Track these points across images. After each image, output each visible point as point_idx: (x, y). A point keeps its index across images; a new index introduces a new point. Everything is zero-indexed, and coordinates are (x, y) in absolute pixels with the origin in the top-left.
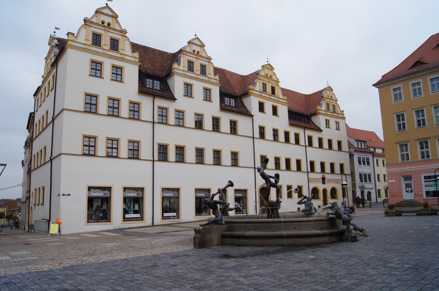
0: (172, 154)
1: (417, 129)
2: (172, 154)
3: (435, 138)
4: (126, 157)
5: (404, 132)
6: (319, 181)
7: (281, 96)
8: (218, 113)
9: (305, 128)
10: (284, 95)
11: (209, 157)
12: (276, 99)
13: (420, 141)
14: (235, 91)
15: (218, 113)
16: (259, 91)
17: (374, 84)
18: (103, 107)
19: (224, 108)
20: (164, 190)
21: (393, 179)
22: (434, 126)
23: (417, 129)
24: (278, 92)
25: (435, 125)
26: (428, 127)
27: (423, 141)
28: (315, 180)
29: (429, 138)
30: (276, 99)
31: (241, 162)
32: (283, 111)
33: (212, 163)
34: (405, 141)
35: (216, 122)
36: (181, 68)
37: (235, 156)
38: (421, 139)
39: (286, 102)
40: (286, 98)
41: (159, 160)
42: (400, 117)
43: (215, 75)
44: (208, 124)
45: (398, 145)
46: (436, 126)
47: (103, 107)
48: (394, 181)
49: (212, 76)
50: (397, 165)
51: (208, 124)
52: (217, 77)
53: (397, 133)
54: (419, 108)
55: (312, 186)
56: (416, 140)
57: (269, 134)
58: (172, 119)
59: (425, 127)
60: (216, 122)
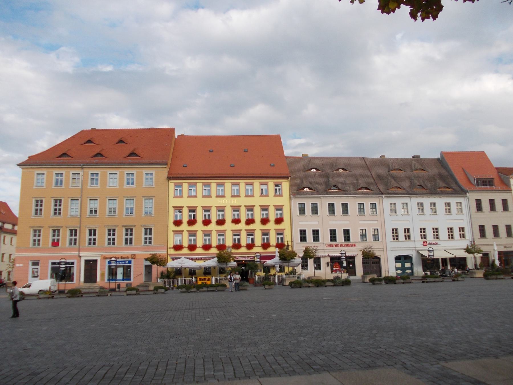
1: (52, 217)
3: (67, 227)
5: (40, 217)
13: (53, 229)
17: (18, 163)
21: (21, 264)
22: (68, 217)
23: (52, 217)
25: (69, 216)
26: (62, 217)
27: (56, 229)
29: (62, 227)
34: (39, 227)
38: (54, 227)
42: (39, 203)
45: (32, 230)
46: (69, 217)
48: (21, 265)
50: (26, 250)
53: (33, 217)
54: (57, 198)
56: (49, 227)
59: (60, 216)
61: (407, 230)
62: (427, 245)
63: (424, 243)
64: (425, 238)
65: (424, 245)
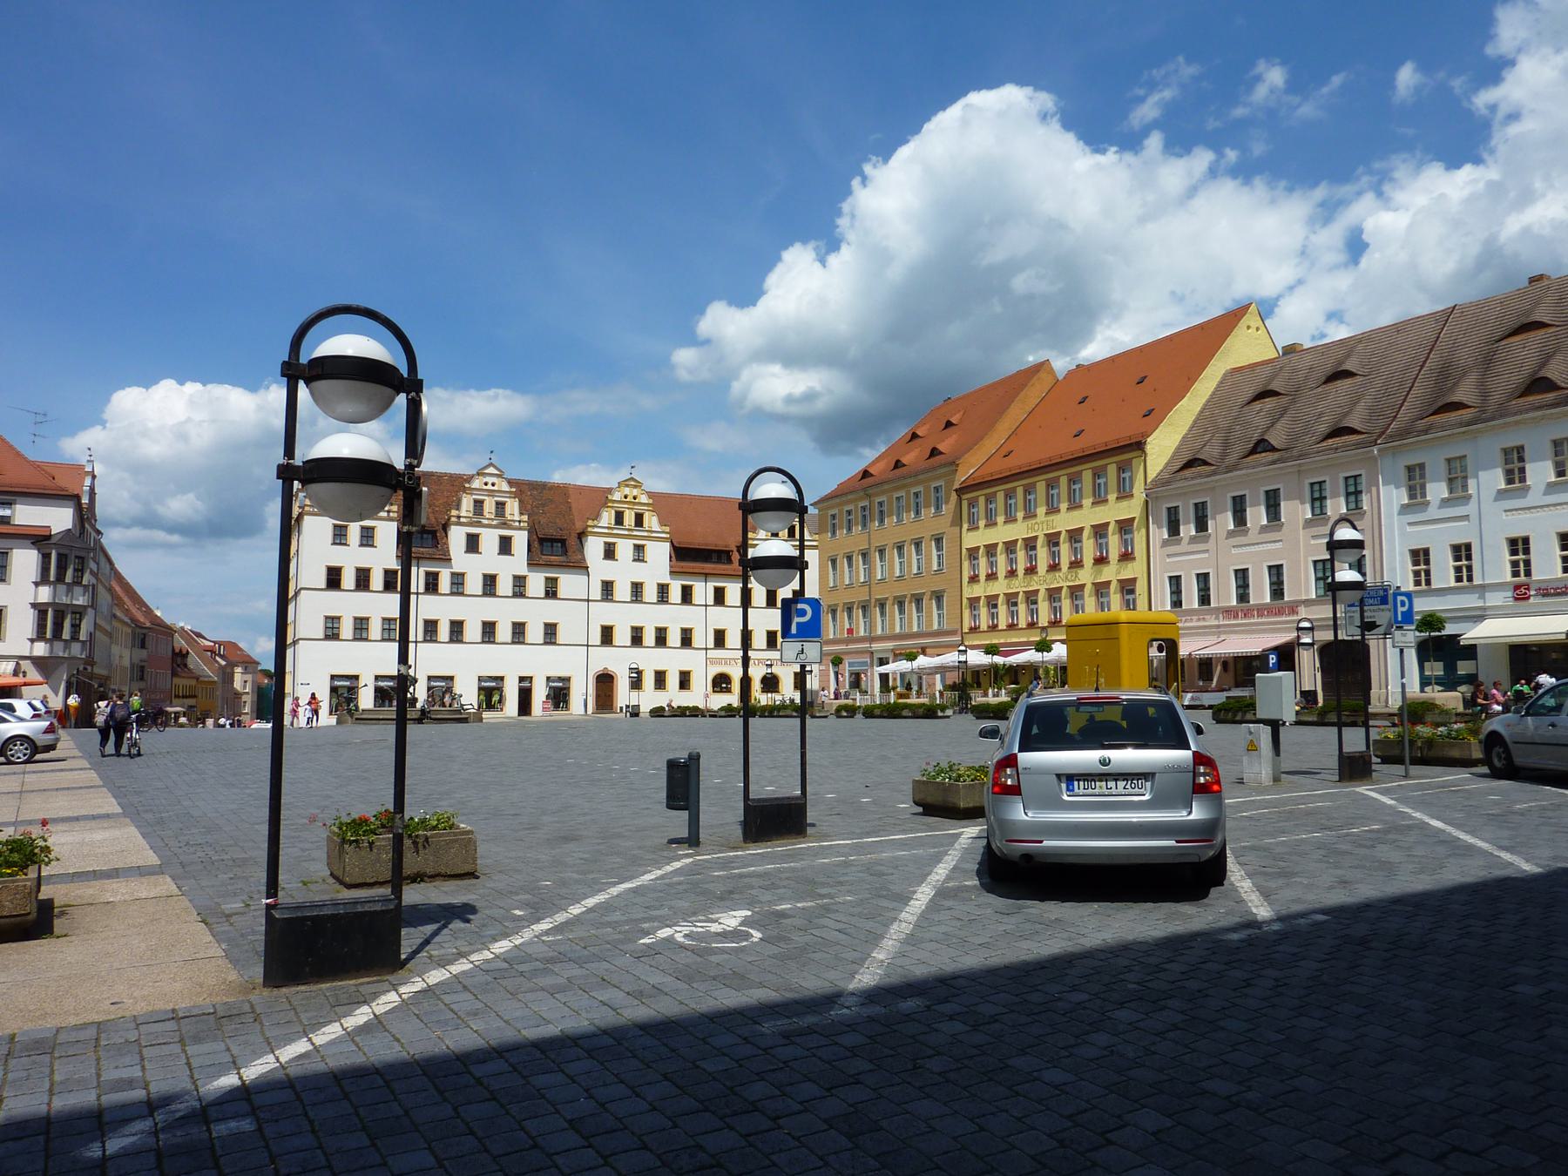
0: (444, 631)
2: (444, 631)
4: (379, 639)
6: (733, 662)
7: (656, 527)
8: (522, 569)
9: (706, 576)
10: (662, 523)
11: (504, 632)
12: (646, 534)
14: (574, 524)
15: (522, 569)
16: (607, 525)
18: (348, 580)
19: (533, 564)
20: (430, 678)
24: (651, 521)
28: (727, 661)
30: (646, 534)
31: (561, 636)
32: (659, 553)
33: (509, 641)
35: (519, 583)
36: (463, 513)
37: (550, 631)
39: (668, 536)
40: (667, 529)
41: (425, 641)
43: (521, 514)
44: (505, 586)
47: (348, 580)
49: (517, 518)
51: (505, 586)
52: (525, 518)
55: (714, 671)
57: (622, 591)
58: (445, 583)
60: (519, 583)
61: (1462, 552)
62: (1528, 598)
63: (1518, 592)
64: (1528, 573)
65: (1516, 599)
